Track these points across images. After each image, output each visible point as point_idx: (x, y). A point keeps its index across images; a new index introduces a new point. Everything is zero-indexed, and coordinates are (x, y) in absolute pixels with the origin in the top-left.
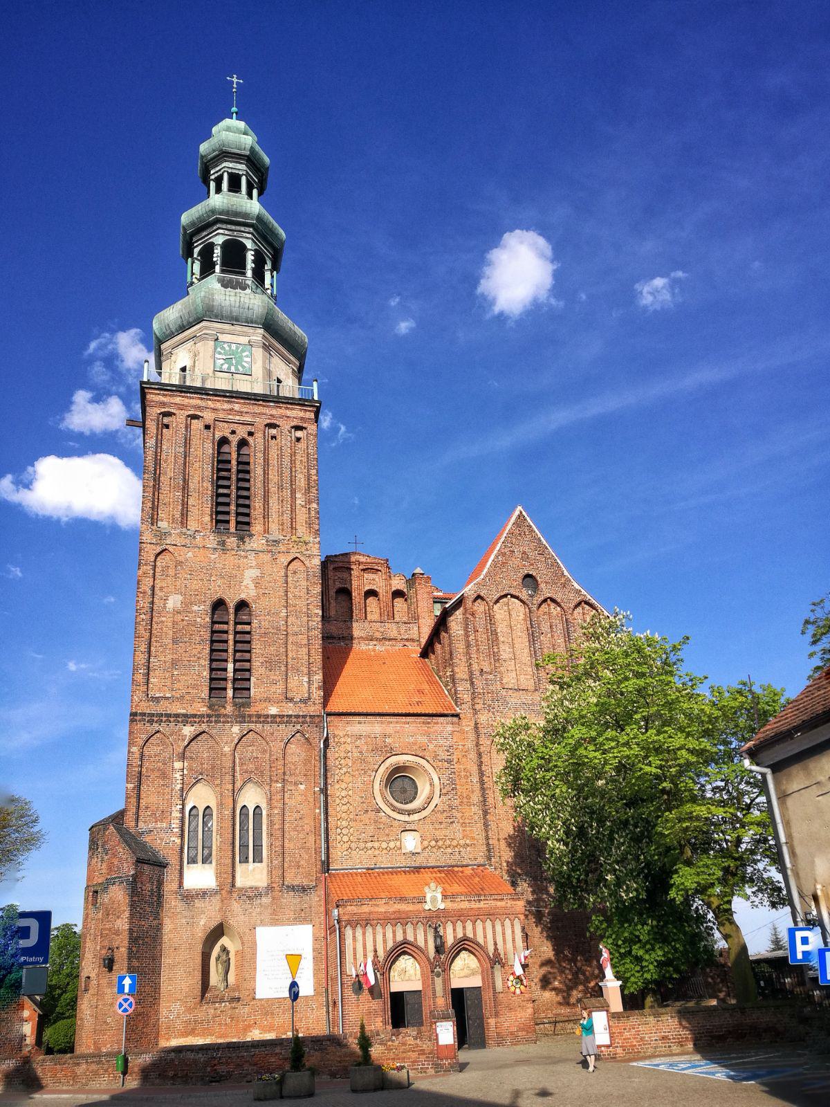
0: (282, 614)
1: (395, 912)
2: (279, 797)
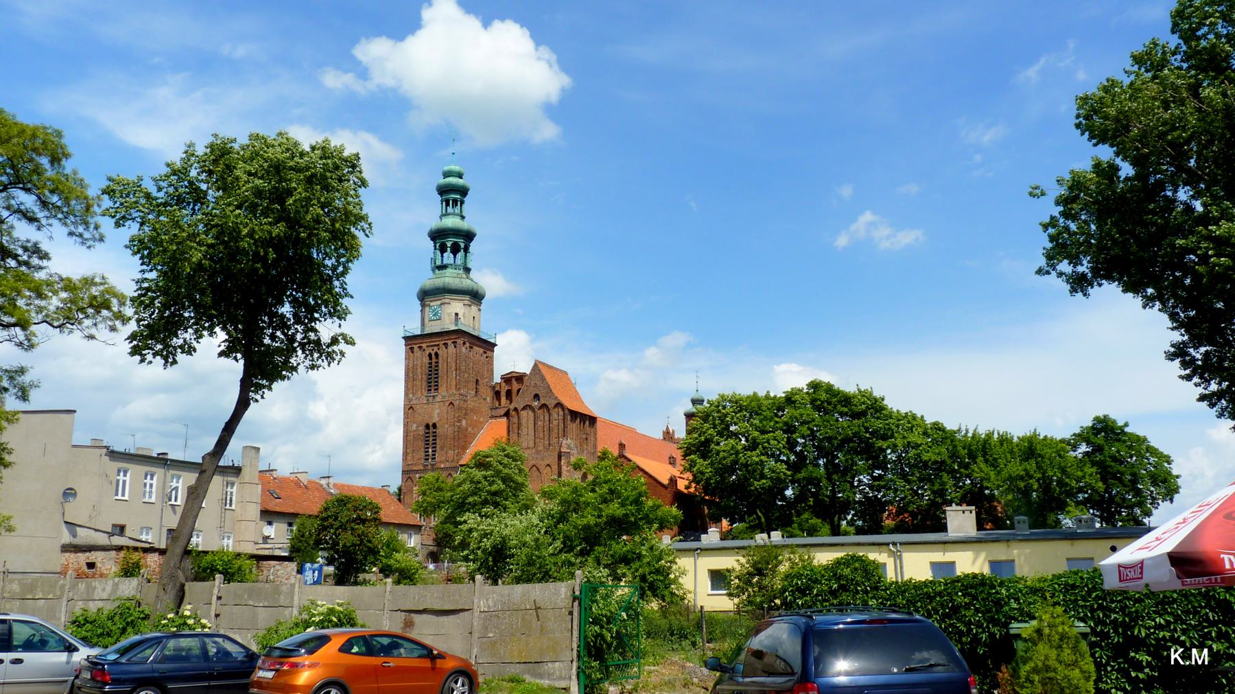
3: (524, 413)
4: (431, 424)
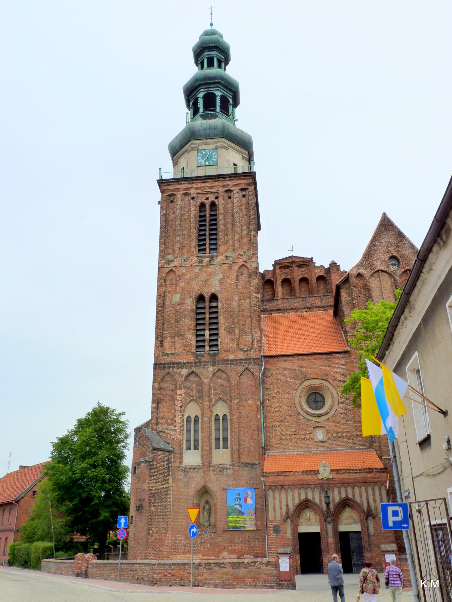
0: (235, 299)
1: (299, 480)
2: (236, 408)
3: (374, 283)
4: (207, 296)
